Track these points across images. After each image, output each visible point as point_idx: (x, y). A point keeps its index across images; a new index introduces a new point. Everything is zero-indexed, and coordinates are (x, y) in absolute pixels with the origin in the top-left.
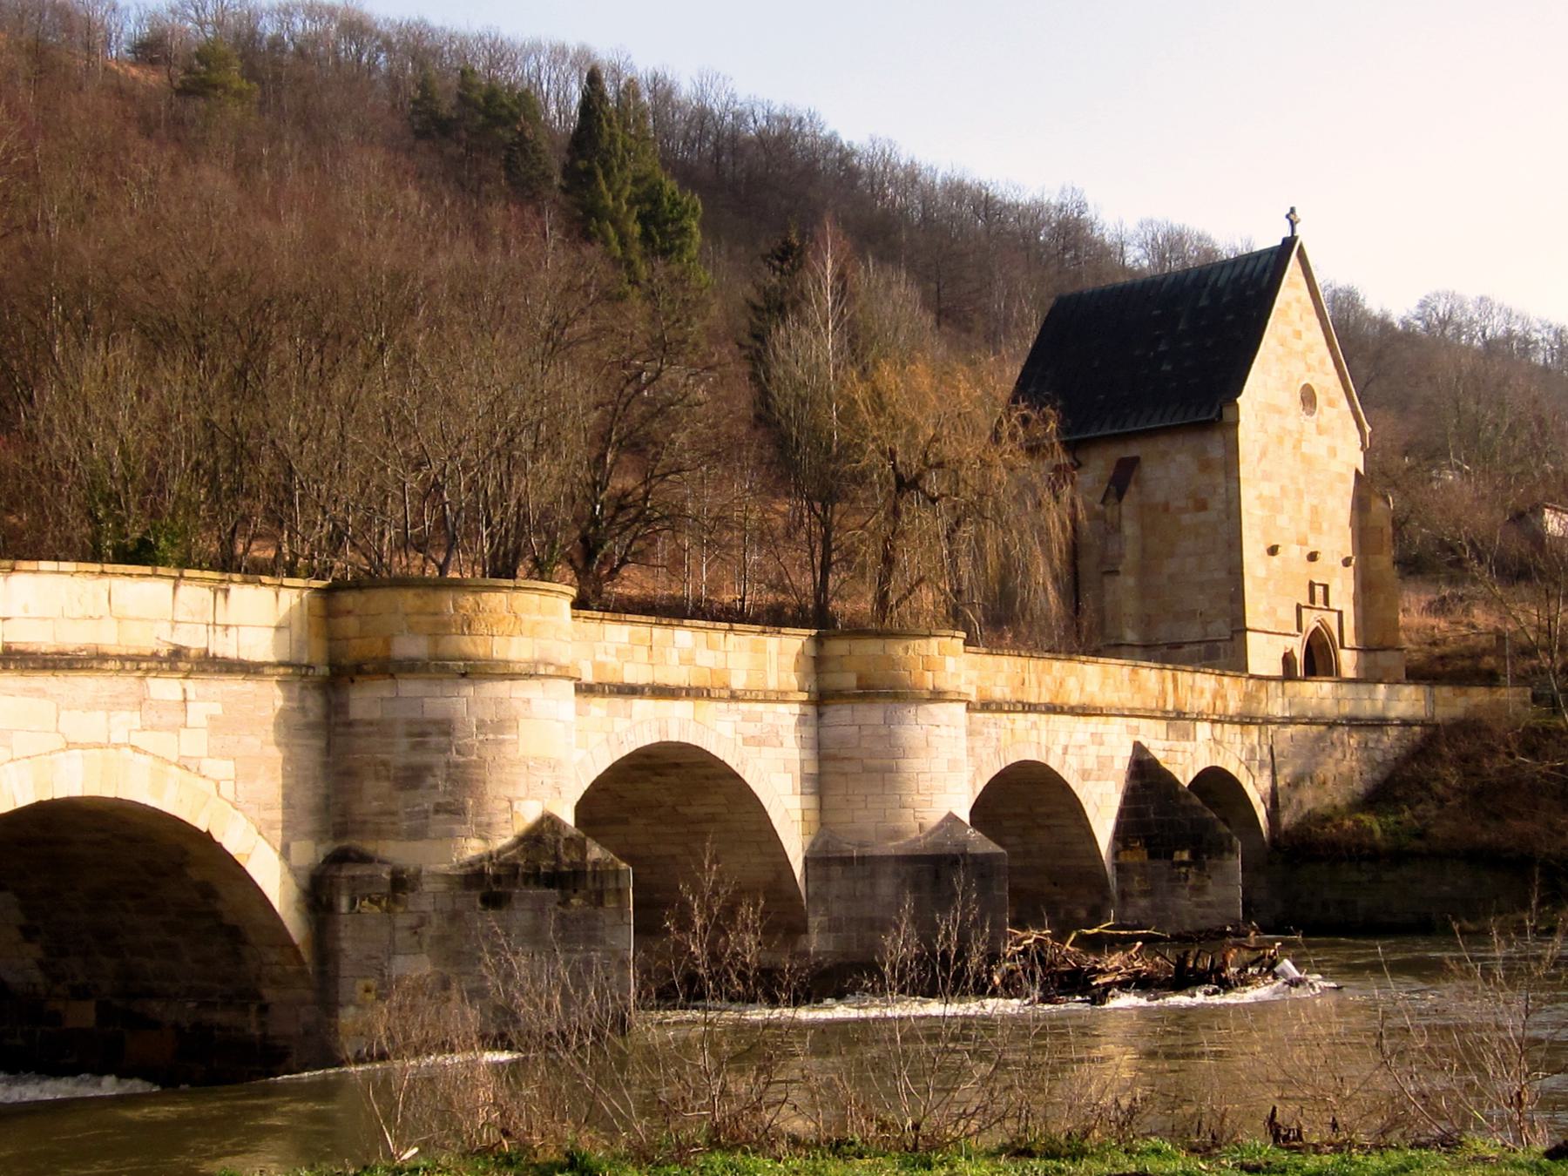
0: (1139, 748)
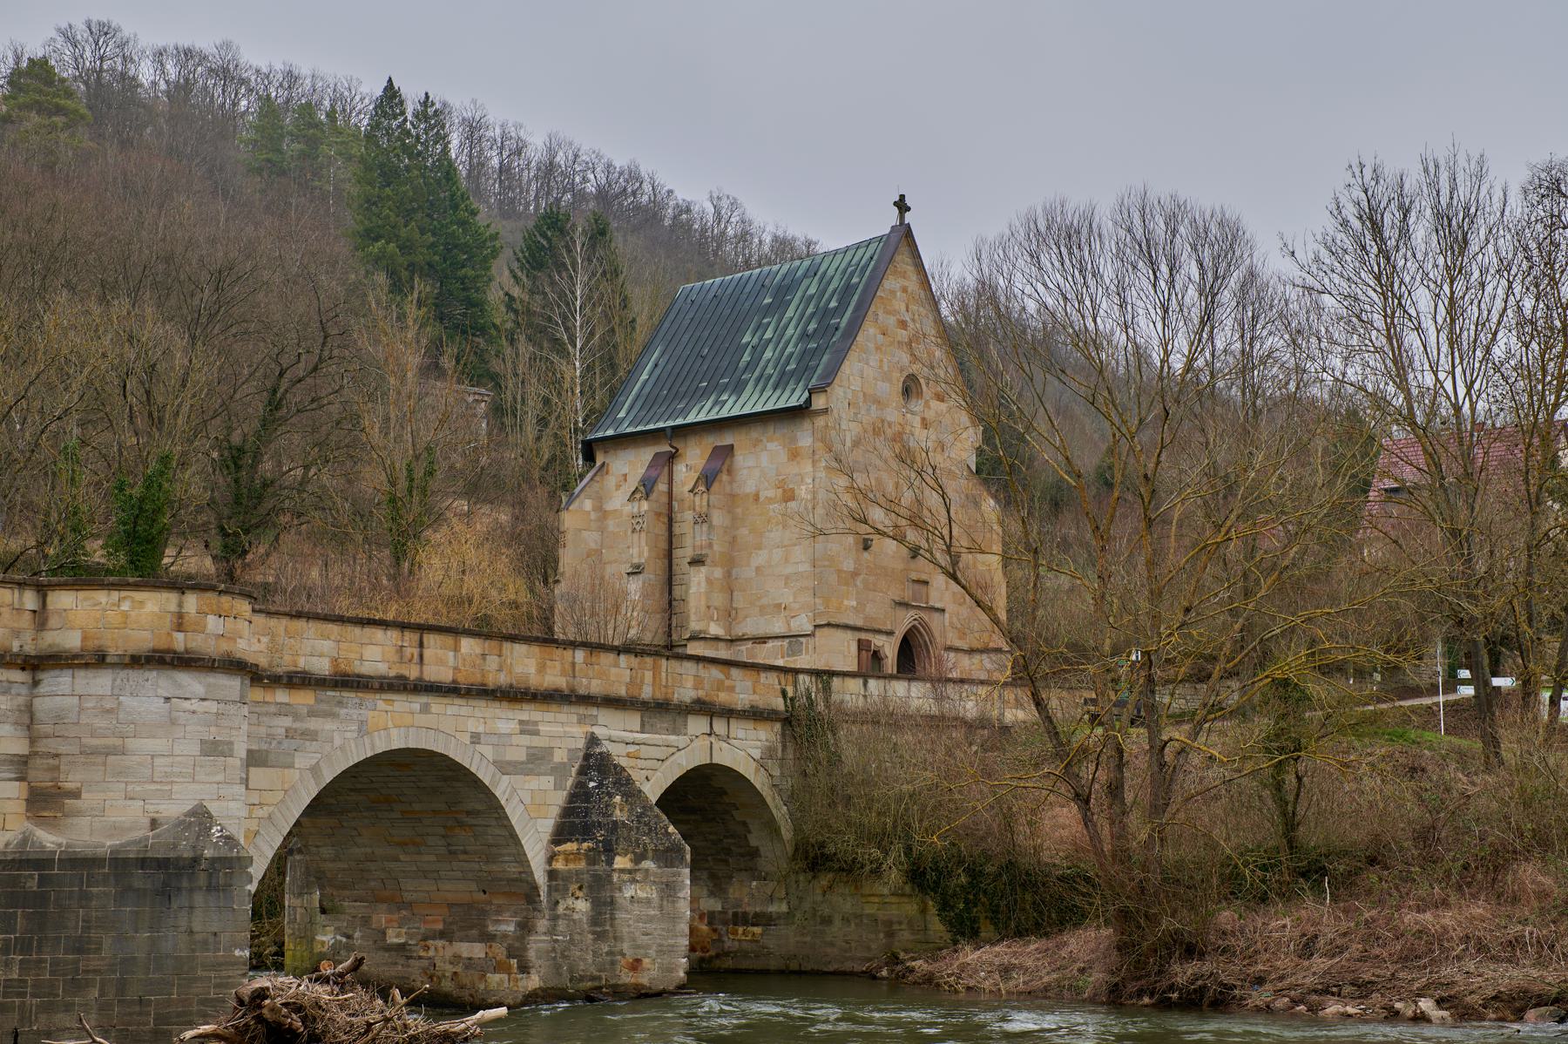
0: (593, 740)
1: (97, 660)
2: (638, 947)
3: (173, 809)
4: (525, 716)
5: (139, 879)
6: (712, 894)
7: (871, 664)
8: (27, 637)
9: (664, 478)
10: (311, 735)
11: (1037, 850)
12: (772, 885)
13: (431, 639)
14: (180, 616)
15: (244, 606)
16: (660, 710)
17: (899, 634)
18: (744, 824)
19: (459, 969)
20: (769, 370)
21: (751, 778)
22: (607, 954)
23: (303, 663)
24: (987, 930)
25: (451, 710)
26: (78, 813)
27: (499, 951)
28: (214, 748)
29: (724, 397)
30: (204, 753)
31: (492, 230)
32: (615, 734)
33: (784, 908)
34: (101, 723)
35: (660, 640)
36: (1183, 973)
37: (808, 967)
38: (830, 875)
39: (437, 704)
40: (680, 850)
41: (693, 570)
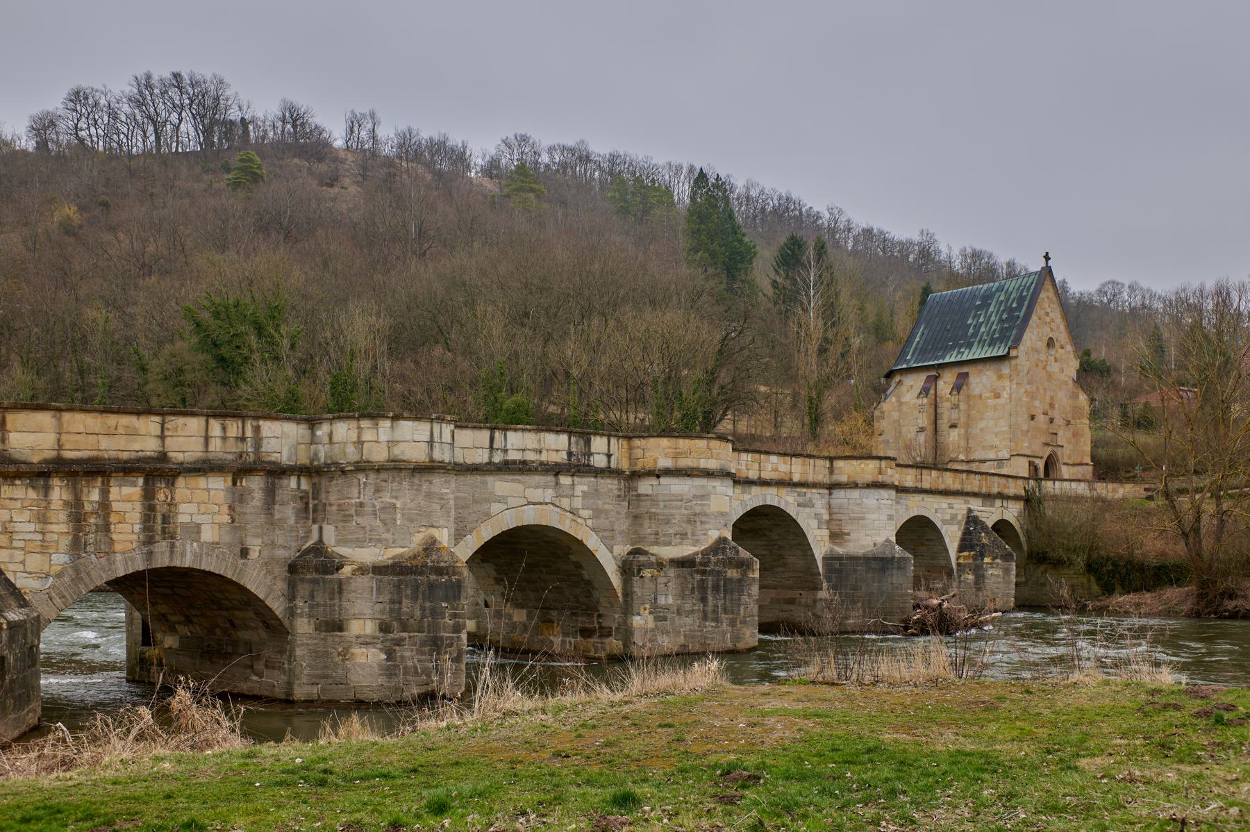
0: (970, 511)
1: (855, 486)
2: (994, 594)
5: (874, 565)
9: (933, 387)
14: (880, 469)
16: (988, 497)
17: (1045, 458)
20: (985, 337)
21: (1014, 524)
25: (930, 500)
26: (849, 541)
29: (963, 350)
30: (889, 519)
31: (752, 244)
34: (856, 508)
36: (1230, 605)
38: (1045, 566)
40: (1012, 555)
41: (951, 430)
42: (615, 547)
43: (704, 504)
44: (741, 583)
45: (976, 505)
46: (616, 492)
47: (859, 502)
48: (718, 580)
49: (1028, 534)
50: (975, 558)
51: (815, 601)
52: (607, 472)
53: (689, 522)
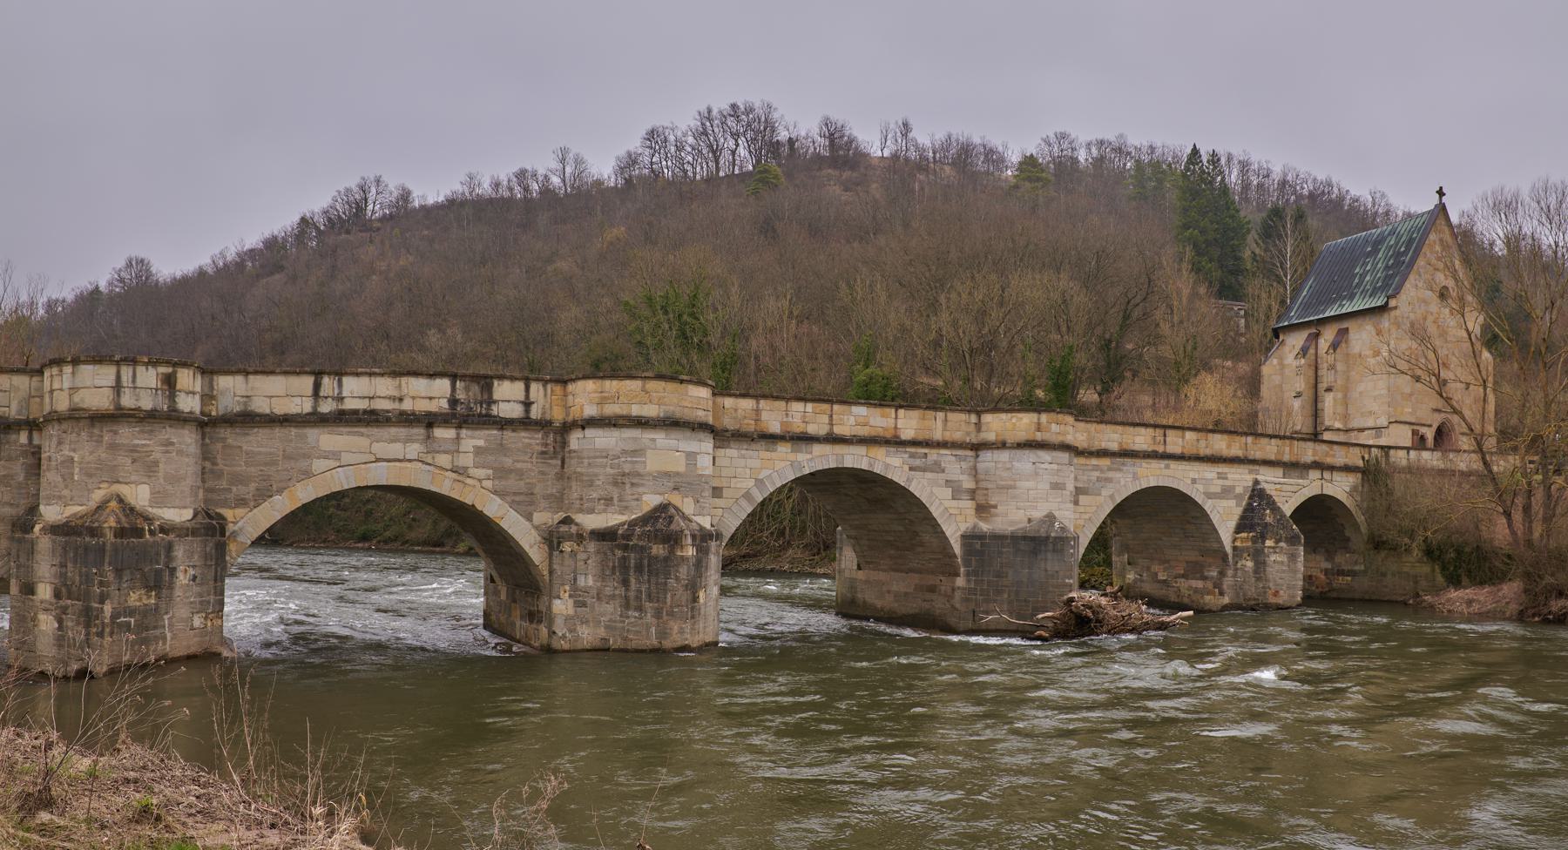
0: (1256, 482)
1: (1002, 445)
3: (1038, 514)
4: (1220, 470)
5: (1023, 546)
6: (1327, 560)
7: (1420, 442)
8: (973, 436)
9: (1313, 346)
10: (1109, 480)
11: (1492, 540)
12: (1357, 556)
13: (1170, 433)
14: (1039, 424)
15: (1070, 419)
16: (1294, 467)
17: (1435, 426)
18: (1342, 525)
19: (1191, 592)
22: (1263, 588)
23: (1104, 445)
24: (1465, 581)
26: (996, 515)
27: (1210, 585)
28: (1057, 486)
30: (1052, 488)
32: (1269, 479)
33: (1362, 568)
34: (1005, 474)
35: (1308, 429)
37: (1374, 597)
39: (1173, 464)
40: (1299, 537)
41: (1327, 394)
42: (535, 514)
43: (636, 462)
44: (669, 562)
45: (1270, 479)
46: (540, 448)
47: (1008, 466)
48: (641, 559)
49: (1370, 513)
50: (1254, 540)
51: (953, 590)
52: (525, 423)
53: (615, 484)
